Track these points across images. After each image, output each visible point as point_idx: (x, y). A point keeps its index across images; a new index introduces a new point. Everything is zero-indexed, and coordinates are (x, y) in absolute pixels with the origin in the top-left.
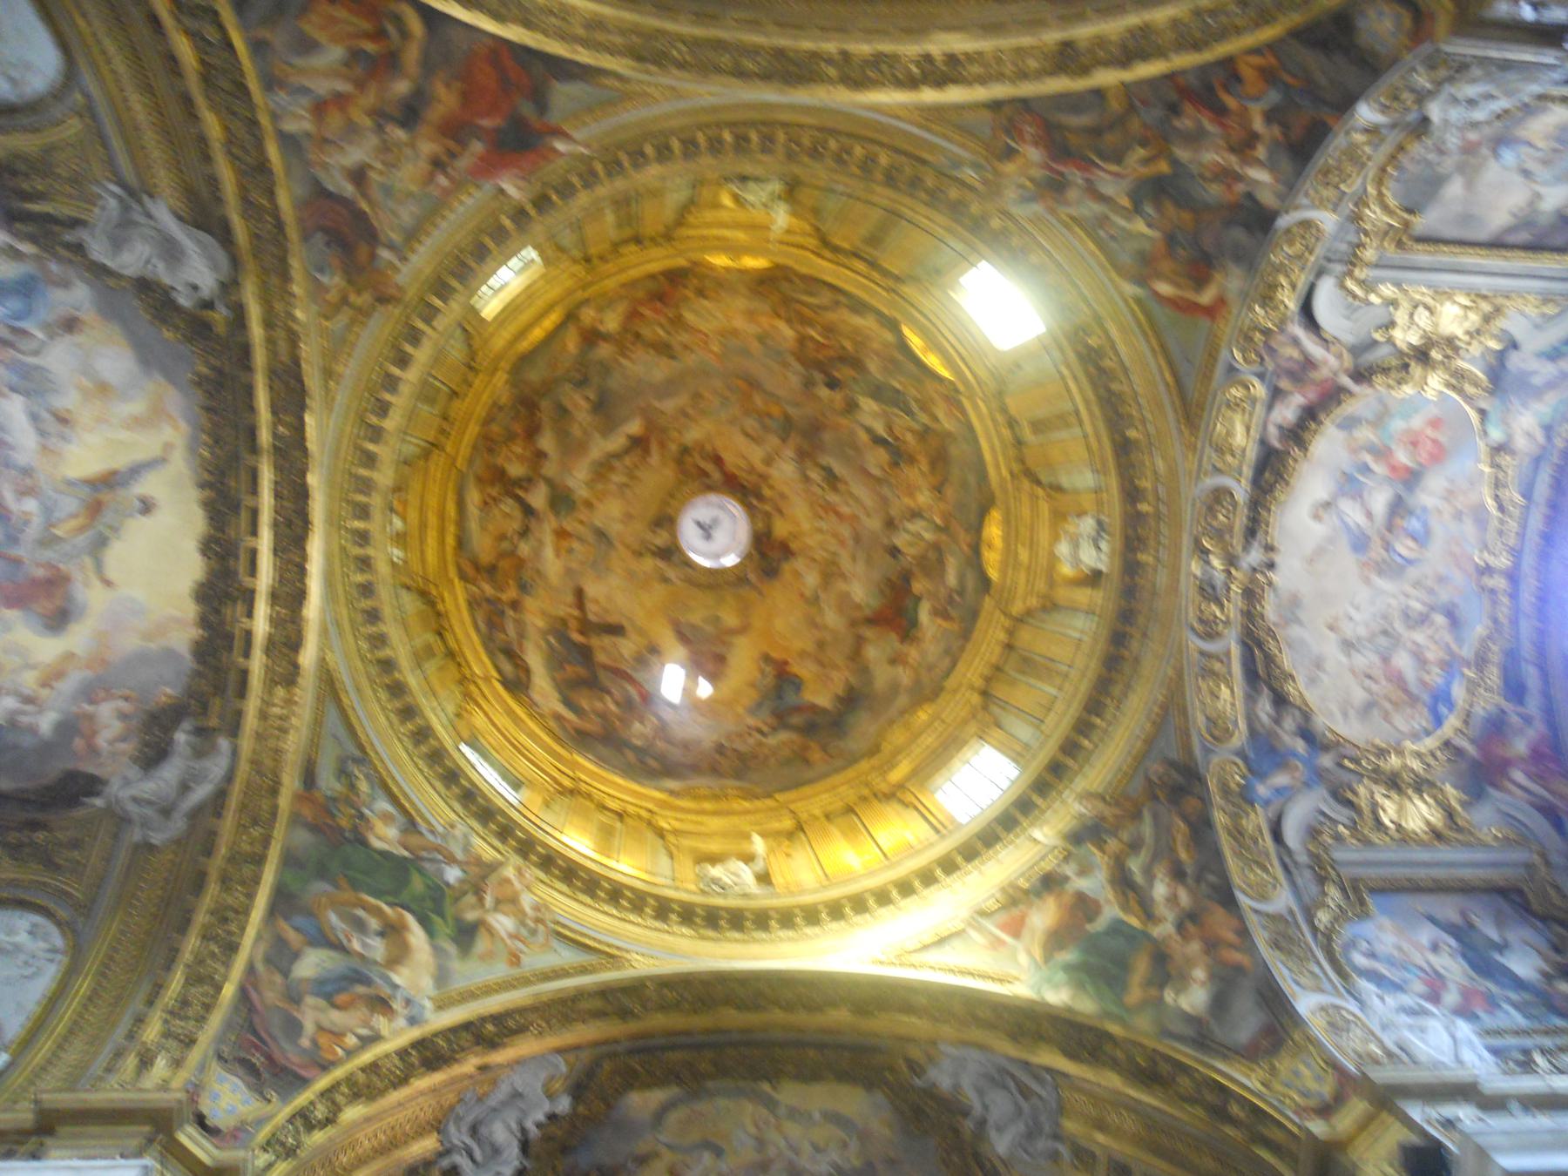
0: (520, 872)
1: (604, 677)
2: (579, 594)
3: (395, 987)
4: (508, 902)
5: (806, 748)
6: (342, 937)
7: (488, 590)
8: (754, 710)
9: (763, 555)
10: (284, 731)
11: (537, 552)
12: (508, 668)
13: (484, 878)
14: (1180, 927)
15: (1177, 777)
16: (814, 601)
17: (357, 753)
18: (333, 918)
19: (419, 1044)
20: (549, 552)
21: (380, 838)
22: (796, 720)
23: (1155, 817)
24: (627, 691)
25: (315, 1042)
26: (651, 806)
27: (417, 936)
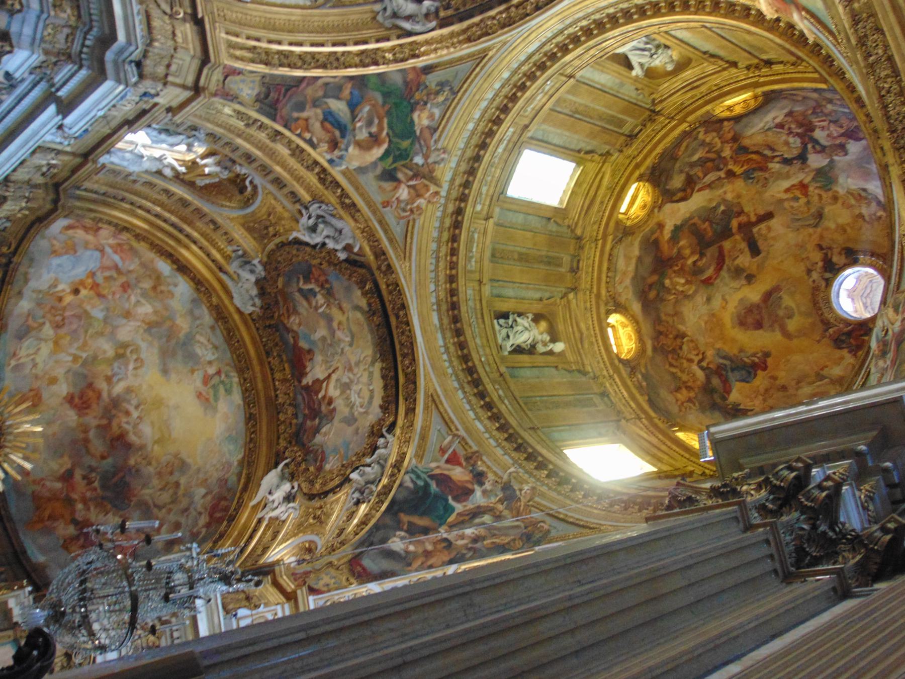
0: (437, 193)
1: (712, 251)
2: (769, 216)
3: (346, 150)
4: (417, 193)
5: (689, 388)
6: (359, 117)
7: (727, 153)
8: (719, 353)
9: (849, 334)
10: (448, 47)
11: (780, 176)
12: (677, 182)
13: (424, 177)
14: (446, 540)
15: (538, 536)
16: (822, 378)
17: (456, 89)
18: (367, 109)
19: (324, 170)
20: (786, 184)
21: (419, 116)
22: (716, 382)
23: (517, 527)
24: (708, 268)
25: (298, 119)
26: (595, 290)
27: (378, 152)
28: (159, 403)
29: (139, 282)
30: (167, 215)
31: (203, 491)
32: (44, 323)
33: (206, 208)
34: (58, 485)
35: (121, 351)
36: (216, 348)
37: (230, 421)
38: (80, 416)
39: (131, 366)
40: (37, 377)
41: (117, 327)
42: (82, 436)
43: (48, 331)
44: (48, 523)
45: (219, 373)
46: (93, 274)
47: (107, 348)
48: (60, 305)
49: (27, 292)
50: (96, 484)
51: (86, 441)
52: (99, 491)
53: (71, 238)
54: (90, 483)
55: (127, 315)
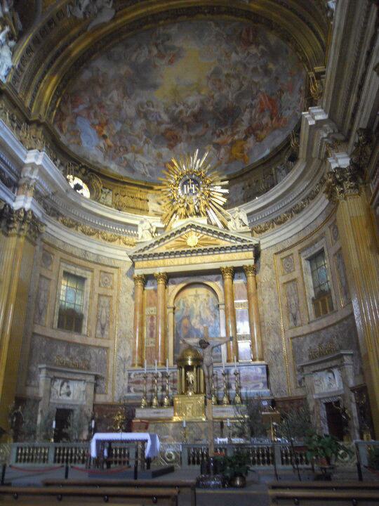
28: (175, 92)
29: (97, 96)
30: (47, 61)
31: (234, 55)
32: (125, 158)
33: (38, 24)
34: (223, 151)
35: (142, 115)
36: (140, 46)
37: (189, 36)
38: (181, 141)
39: (152, 109)
40: (158, 164)
41: (127, 115)
42: (193, 140)
43: (129, 156)
44: (245, 153)
45: (157, 45)
46: (93, 125)
47: (139, 124)
48: (113, 148)
49: (106, 163)
50: (223, 129)
51: (196, 137)
52: (227, 127)
53: (68, 131)
54: (222, 133)
55: (119, 108)
